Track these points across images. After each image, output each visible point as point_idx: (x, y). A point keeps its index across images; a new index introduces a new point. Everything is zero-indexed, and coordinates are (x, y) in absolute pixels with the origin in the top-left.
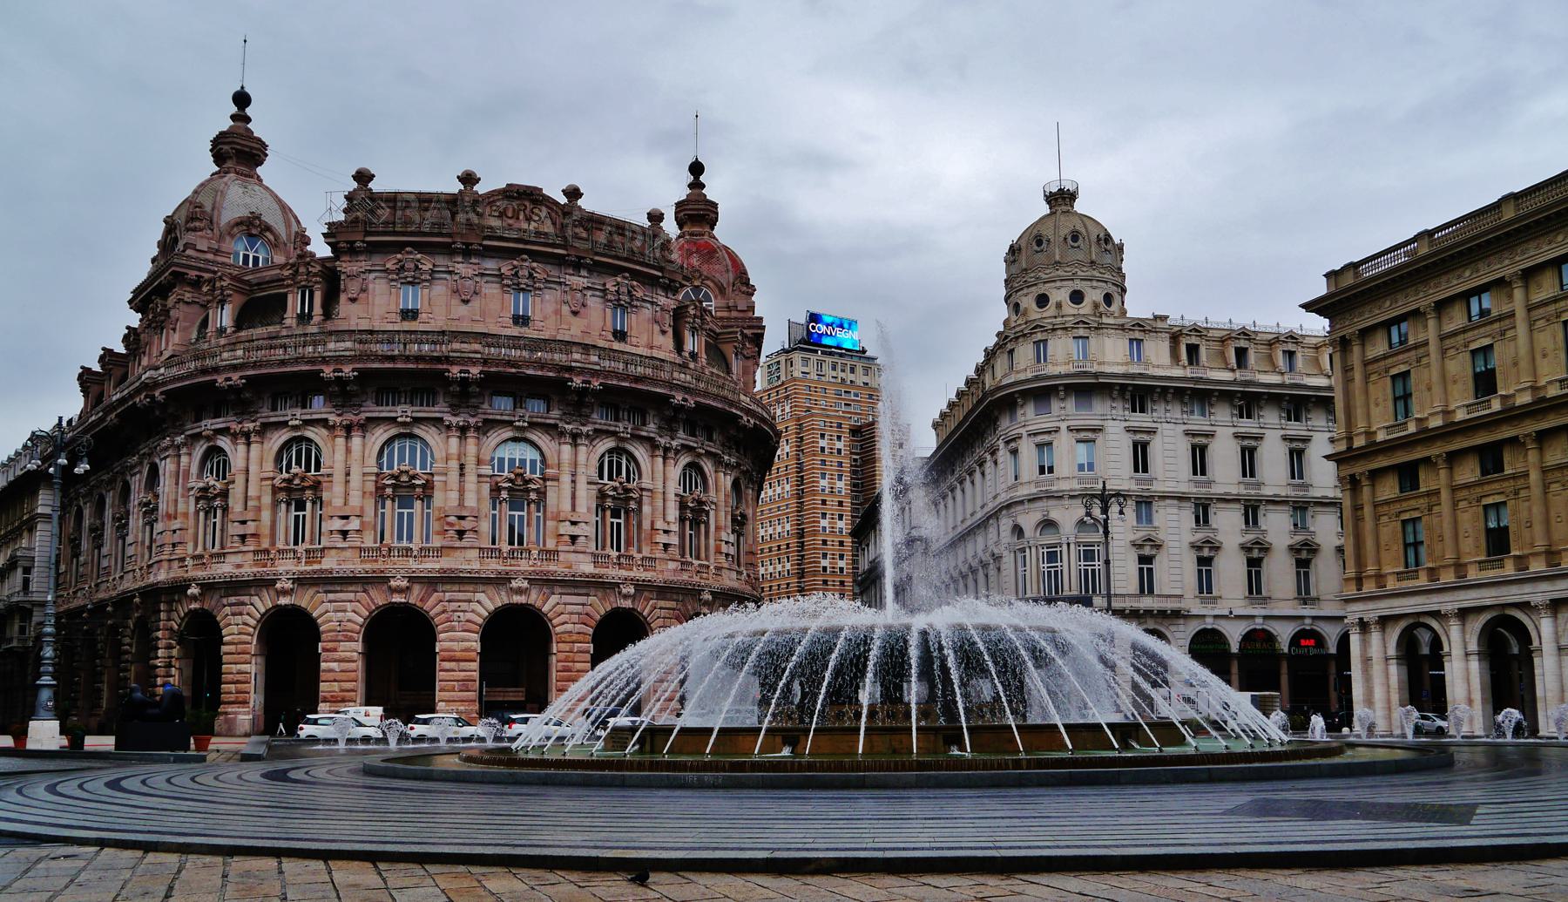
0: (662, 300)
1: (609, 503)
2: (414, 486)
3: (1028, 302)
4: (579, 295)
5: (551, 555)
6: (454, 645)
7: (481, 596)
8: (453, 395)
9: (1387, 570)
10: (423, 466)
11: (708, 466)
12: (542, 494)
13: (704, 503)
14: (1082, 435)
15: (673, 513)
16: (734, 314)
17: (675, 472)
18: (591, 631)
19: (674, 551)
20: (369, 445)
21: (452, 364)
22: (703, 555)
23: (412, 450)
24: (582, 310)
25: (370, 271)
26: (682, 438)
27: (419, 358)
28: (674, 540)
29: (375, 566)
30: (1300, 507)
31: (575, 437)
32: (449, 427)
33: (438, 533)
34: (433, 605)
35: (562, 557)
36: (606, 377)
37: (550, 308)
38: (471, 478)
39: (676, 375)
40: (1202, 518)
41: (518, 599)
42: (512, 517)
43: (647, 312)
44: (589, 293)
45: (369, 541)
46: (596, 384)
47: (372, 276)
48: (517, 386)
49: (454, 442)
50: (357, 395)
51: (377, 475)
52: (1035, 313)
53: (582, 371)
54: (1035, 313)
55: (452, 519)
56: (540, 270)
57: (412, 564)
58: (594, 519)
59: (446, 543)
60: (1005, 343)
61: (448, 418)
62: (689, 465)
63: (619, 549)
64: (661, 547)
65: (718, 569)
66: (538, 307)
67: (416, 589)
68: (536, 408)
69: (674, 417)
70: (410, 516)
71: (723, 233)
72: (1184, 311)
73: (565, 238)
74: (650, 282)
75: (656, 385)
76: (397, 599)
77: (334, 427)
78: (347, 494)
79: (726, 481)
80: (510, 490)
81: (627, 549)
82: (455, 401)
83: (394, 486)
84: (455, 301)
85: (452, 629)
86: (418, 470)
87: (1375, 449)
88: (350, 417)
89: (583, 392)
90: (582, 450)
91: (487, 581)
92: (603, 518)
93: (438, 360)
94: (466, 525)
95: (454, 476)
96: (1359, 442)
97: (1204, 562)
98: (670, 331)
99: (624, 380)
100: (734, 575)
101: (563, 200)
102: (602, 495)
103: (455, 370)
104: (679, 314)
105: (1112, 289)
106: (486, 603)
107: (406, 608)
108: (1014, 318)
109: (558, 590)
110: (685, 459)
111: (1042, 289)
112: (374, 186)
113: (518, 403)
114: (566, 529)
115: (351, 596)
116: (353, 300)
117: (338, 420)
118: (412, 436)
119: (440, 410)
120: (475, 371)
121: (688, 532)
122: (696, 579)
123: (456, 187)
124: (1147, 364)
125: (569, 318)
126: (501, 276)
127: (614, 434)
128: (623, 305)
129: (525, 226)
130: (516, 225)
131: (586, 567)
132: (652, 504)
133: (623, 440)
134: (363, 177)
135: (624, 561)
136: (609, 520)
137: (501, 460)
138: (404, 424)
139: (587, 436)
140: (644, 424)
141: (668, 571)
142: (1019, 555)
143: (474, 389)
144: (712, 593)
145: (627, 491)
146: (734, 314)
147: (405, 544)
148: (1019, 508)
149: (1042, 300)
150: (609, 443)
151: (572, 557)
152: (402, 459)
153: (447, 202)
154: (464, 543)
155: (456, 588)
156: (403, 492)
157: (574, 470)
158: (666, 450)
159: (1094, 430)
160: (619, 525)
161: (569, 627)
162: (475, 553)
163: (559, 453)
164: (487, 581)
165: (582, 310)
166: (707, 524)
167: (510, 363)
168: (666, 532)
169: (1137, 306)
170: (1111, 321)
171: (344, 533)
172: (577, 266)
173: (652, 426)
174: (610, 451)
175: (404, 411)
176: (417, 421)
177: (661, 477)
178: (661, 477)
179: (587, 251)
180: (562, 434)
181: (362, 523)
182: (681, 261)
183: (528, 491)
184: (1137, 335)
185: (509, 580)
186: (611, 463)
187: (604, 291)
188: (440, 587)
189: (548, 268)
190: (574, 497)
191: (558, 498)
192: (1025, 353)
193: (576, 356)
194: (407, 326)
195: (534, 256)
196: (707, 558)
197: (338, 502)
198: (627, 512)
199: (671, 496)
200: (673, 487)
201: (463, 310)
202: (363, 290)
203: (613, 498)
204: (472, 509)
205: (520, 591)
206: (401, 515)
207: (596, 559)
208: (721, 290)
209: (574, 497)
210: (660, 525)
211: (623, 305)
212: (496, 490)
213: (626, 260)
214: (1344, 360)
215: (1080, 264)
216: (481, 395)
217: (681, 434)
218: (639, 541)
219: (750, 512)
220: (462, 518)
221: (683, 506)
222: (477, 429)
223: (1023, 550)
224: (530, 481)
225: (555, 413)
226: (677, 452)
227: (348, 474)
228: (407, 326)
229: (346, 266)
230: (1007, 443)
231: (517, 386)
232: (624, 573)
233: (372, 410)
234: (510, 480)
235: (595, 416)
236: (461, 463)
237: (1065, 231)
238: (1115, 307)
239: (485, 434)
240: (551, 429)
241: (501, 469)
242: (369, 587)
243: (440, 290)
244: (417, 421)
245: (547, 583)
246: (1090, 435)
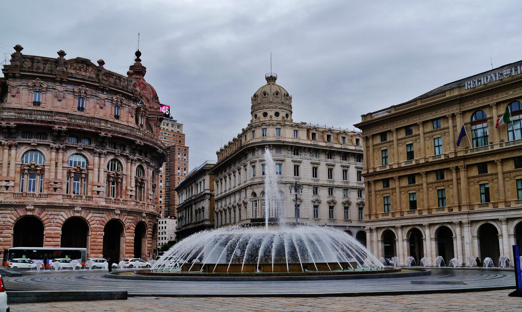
0: (132, 105)
1: (111, 179)
2: (37, 170)
3: (260, 114)
5: (90, 198)
6: (51, 232)
8: (54, 136)
9: (379, 212)
10: (40, 162)
11: (145, 167)
12: (87, 175)
13: (144, 180)
14: (278, 162)
15: (133, 184)
16: (152, 110)
17: (134, 168)
18: (104, 227)
19: (133, 198)
20: (19, 153)
21: (56, 124)
23: (36, 156)
24: (104, 107)
25: (21, 86)
27: (42, 121)
28: (133, 194)
29: (20, 200)
30: (346, 189)
31: (100, 154)
32: (52, 148)
33: (46, 189)
34: (43, 216)
36: (113, 133)
37: (92, 105)
38: (60, 168)
39: (137, 133)
40: (315, 192)
41: (77, 215)
42: (75, 183)
43: (126, 109)
44: (106, 101)
45: (17, 190)
46: (110, 135)
47: (22, 87)
48: (78, 134)
49: (54, 154)
50: (14, 134)
51: (21, 165)
52: (262, 119)
53: (105, 130)
54: (262, 119)
55: (52, 183)
56: (89, 91)
57: (36, 200)
58: (105, 185)
59: (49, 193)
60: (251, 128)
61: (52, 145)
62: (139, 166)
63: (113, 197)
65: (148, 205)
66: (88, 104)
67: (37, 210)
68: (85, 143)
69: (136, 148)
70: (34, 181)
71: (148, 78)
72: (312, 121)
73: (99, 80)
74: (129, 98)
75: (131, 137)
76: (29, 213)
77: (4, 145)
78: (8, 172)
79: (151, 172)
80: (75, 173)
81: (117, 197)
82: (55, 139)
83: (28, 170)
84: (56, 100)
85: (51, 226)
86: (38, 164)
87: (375, 174)
88: (10, 142)
89: (104, 138)
90: (103, 159)
91: (65, 208)
92: (109, 185)
93: (50, 122)
94: (58, 186)
95: (53, 167)
96: (371, 171)
97: (316, 207)
98: (134, 116)
99: (120, 134)
100: (152, 207)
101: (98, 65)
102: (109, 176)
103: (57, 127)
104: (138, 110)
105: (289, 112)
106: (64, 216)
107: (33, 217)
108: (255, 119)
110: (138, 164)
111: (265, 110)
112: (23, 52)
113: (79, 140)
114: (96, 189)
115: (9, 212)
116: (13, 96)
117: (6, 143)
118: (36, 150)
119: (49, 141)
120: (64, 127)
121: (138, 191)
122: (141, 208)
123: (57, 56)
124: (299, 139)
125: (99, 109)
126: (74, 92)
127: (114, 154)
128: (118, 106)
129: (84, 74)
130: (80, 73)
131: (103, 203)
132: (126, 180)
133: (117, 156)
134: (18, 48)
135: (117, 201)
136: (111, 185)
137: (71, 162)
138: (34, 146)
139: (105, 154)
140: (124, 150)
141: (131, 205)
142: (254, 203)
143: (63, 134)
144: (146, 214)
145: (118, 175)
146: (152, 110)
147: (32, 192)
148: (255, 186)
149: (265, 115)
150: (112, 157)
151: (98, 199)
152: (31, 160)
153: (54, 62)
154: (56, 193)
155: (53, 210)
156: (32, 172)
157: (99, 166)
158: (132, 160)
159: (282, 161)
160: (114, 187)
161: (96, 225)
162: (61, 197)
163: (94, 160)
164: (65, 208)
165: (104, 107)
166: (144, 188)
167: (78, 126)
168: (131, 191)
169: (296, 118)
170: (288, 123)
171: (7, 187)
172: (103, 90)
173: (127, 151)
174: (112, 160)
175: (34, 141)
176: (39, 145)
177: (129, 170)
178: (129, 170)
179: (107, 85)
180: (95, 153)
181: (15, 184)
182: (132, 88)
183: (81, 174)
184: (297, 129)
185: (74, 207)
186: (112, 164)
187: (112, 100)
188: (47, 209)
189: (92, 90)
190: (99, 177)
191: (93, 177)
192: (259, 132)
193: (103, 124)
194: (35, 108)
195: (87, 85)
196: (144, 201)
197: (5, 175)
198: (117, 183)
199: (133, 178)
200: (134, 174)
201: (59, 104)
202: (18, 93)
203: (113, 177)
204: (60, 180)
205: (78, 212)
206: (30, 181)
208: (148, 101)
209: (99, 177)
210: (129, 188)
211: (118, 106)
212: (69, 173)
213: (121, 89)
214: (366, 144)
215: (278, 103)
216: (65, 137)
217: (137, 155)
218: (121, 193)
219: (156, 183)
220: (56, 183)
221: (136, 181)
222: (63, 149)
223: (256, 201)
224: (83, 170)
225: (93, 145)
226: (136, 161)
227: (9, 164)
228: (35, 108)
229: (11, 83)
230: (251, 163)
231: (78, 134)
232: (116, 206)
233: (20, 139)
234: (75, 169)
235: (107, 147)
236: (56, 162)
237: (274, 91)
238: (289, 119)
239: (66, 151)
241: (71, 165)
242: (17, 209)
243: (49, 95)
244: (39, 145)
245: (88, 209)
246: (280, 162)
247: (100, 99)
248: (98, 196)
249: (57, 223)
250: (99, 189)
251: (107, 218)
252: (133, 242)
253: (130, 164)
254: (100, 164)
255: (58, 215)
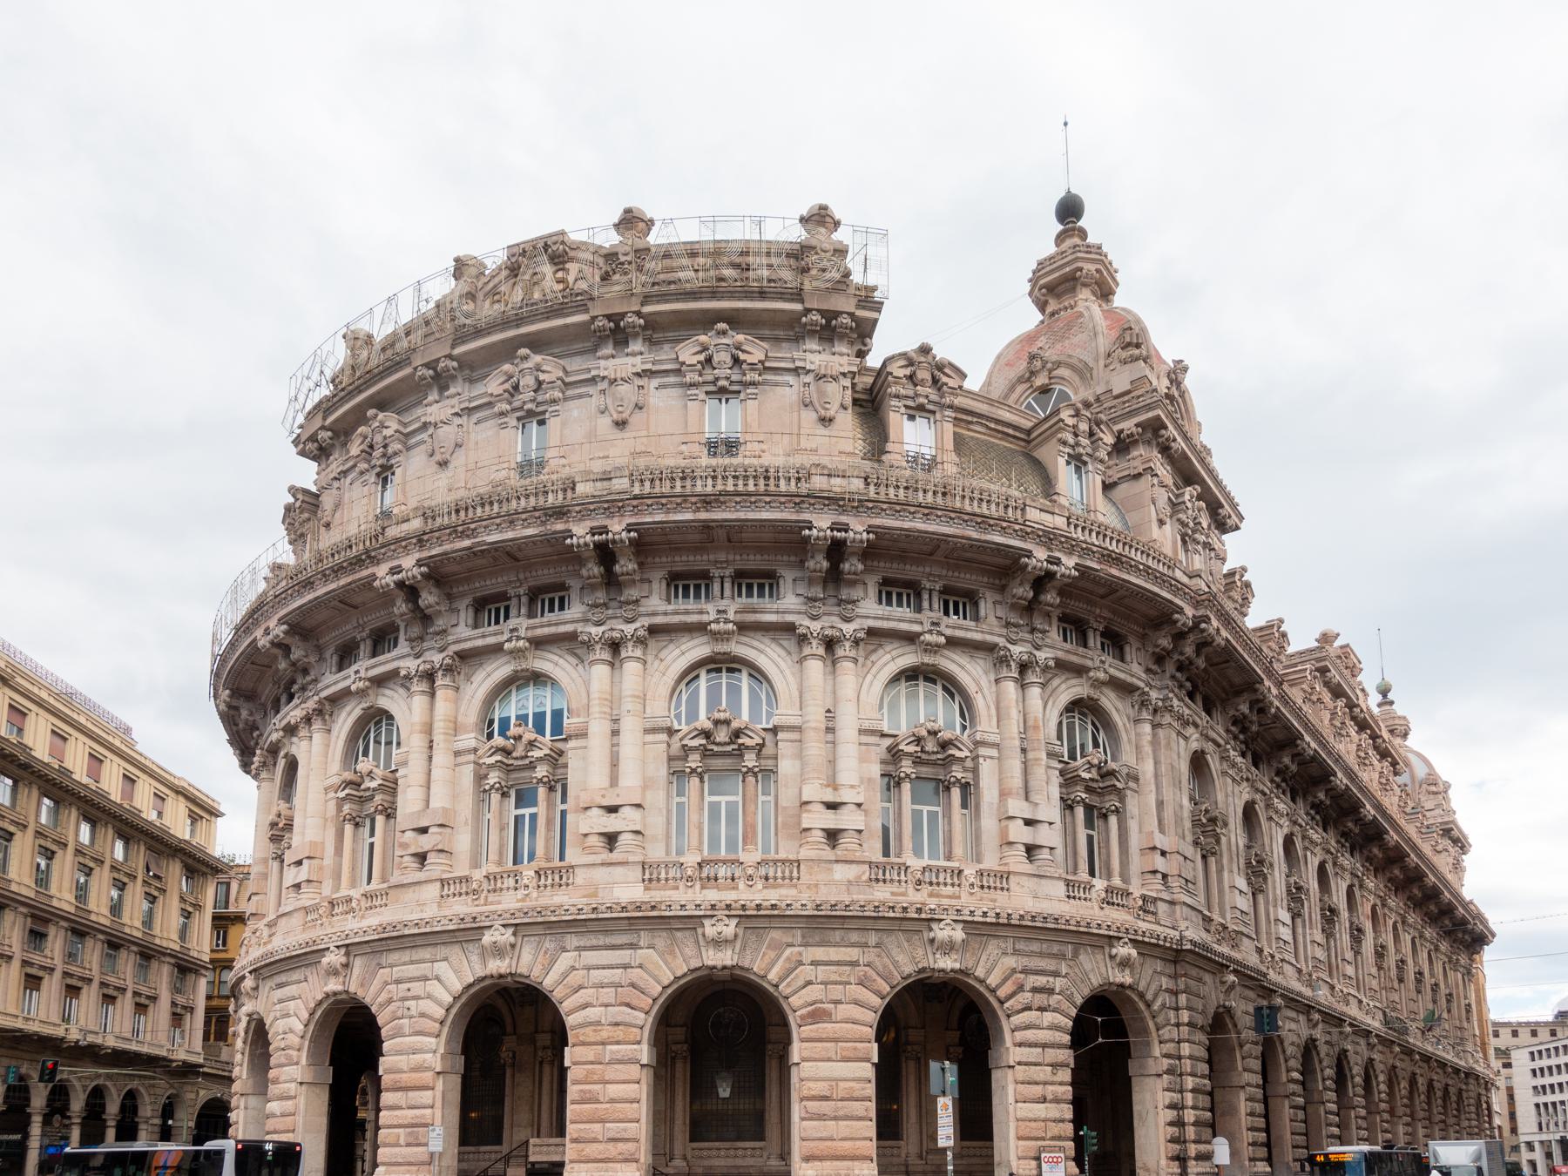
4: (623, 389)
7: (442, 968)
22: (958, 850)
26: (871, 610)
31: (615, 646)
35: (580, 877)
41: (497, 966)
43: (787, 392)
44: (655, 382)
64: (818, 836)
90: (631, 668)
106: (450, 978)
109: (572, 941)
122: (914, 897)
127: (701, 628)
131: (626, 890)
132: (800, 756)
141: (835, 883)
150: (697, 649)
151: (600, 874)
155: (406, 956)
161: (593, 1013)
162: (433, 890)
165: (637, 419)
168: (832, 806)
190: (614, 764)
191: (587, 771)
205: (498, 951)
207: (650, 873)
209: (614, 764)
225: (575, 610)
232: (712, 895)
240: (569, 642)
247: (613, 382)
248: (605, 856)
249: (423, 1015)
250: (611, 823)
251: (662, 967)
252: (871, 1090)
253: (815, 668)
254: (613, 700)
255: (426, 979)
